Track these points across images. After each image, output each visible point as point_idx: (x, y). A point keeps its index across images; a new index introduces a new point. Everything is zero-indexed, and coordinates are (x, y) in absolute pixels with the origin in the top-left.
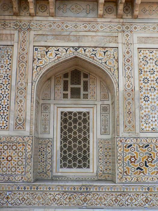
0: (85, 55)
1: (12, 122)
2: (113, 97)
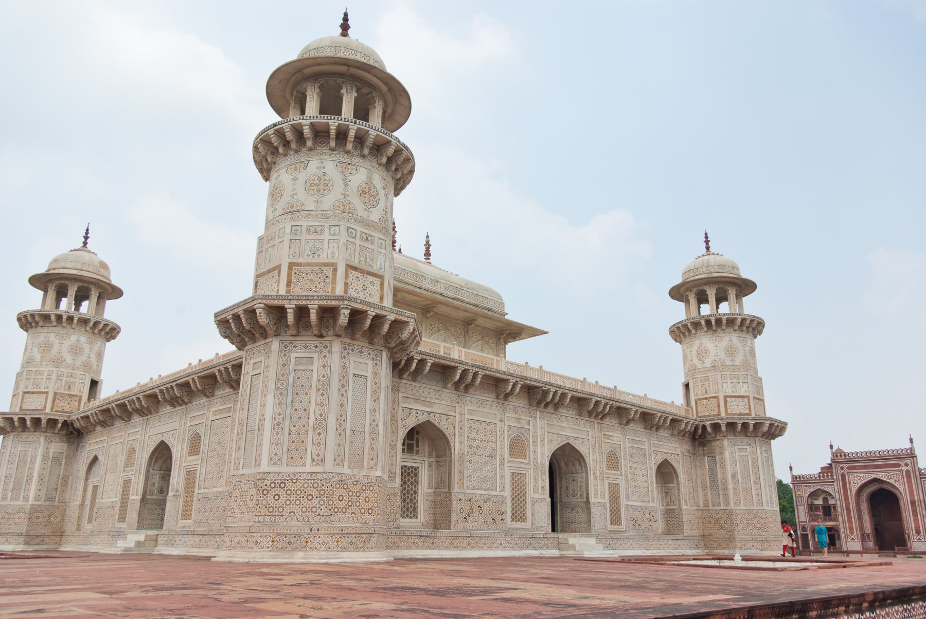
0: (435, 420)
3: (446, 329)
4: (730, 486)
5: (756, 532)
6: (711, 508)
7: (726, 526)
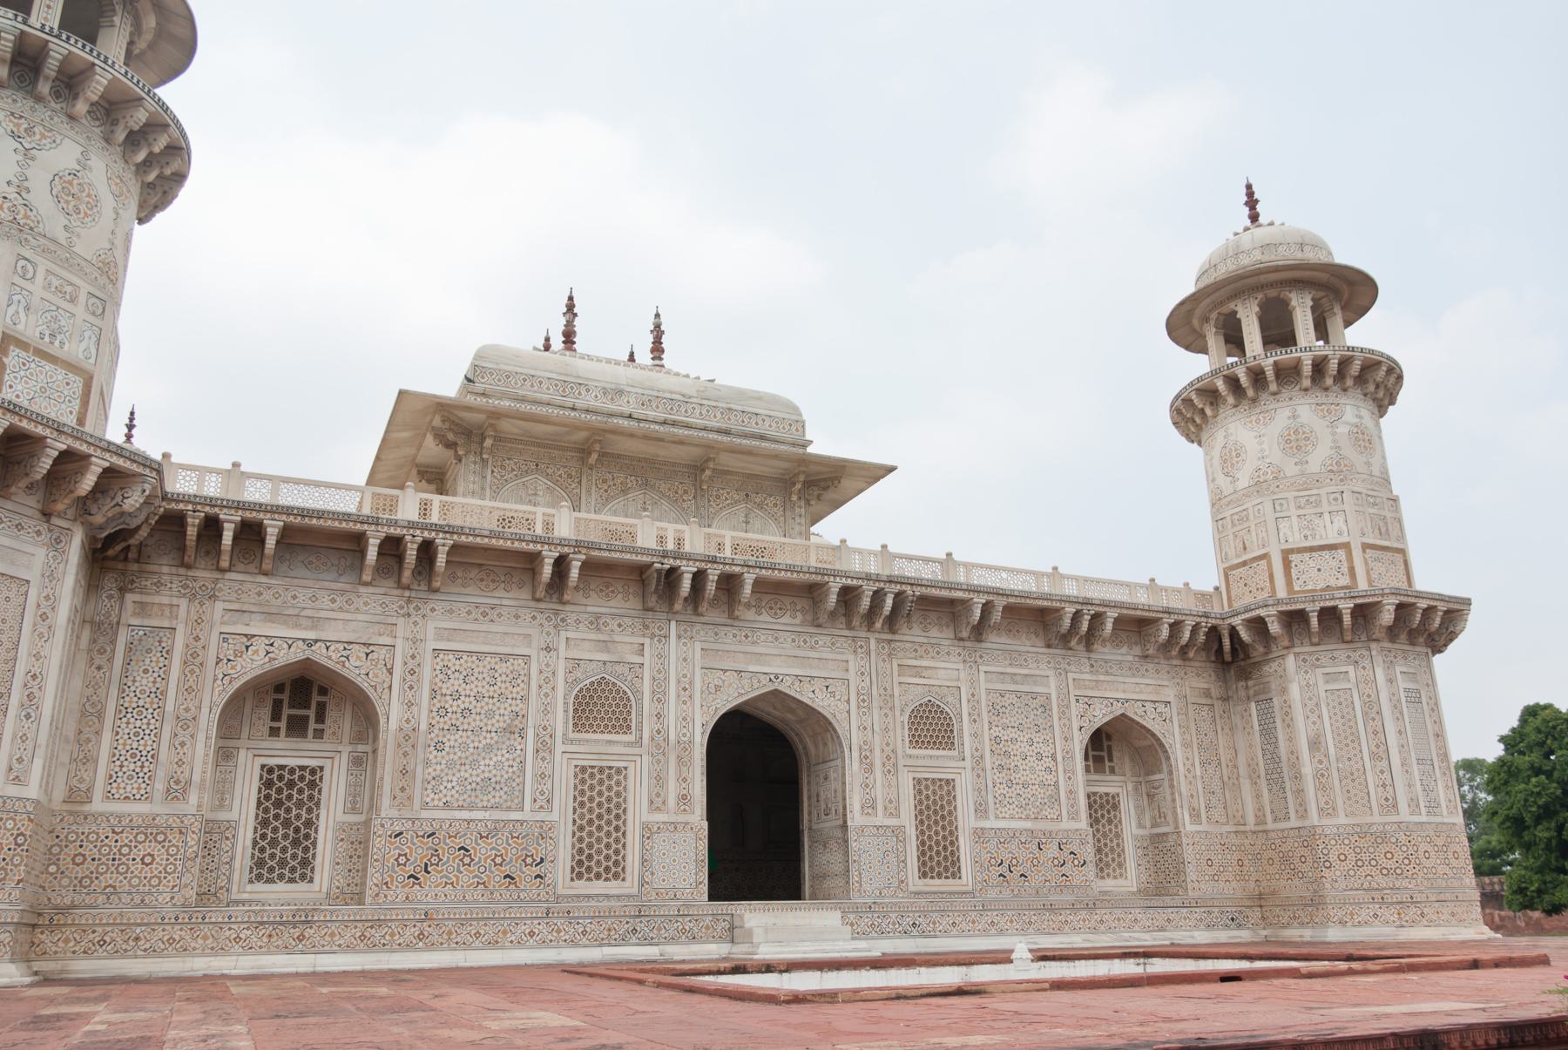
1: (160, 786)
2: (375, 739)
3: (646, 484)
4: (1307, 770)
5: (1383, 882)
6: (1270, 826)
7: (1304, 868)
